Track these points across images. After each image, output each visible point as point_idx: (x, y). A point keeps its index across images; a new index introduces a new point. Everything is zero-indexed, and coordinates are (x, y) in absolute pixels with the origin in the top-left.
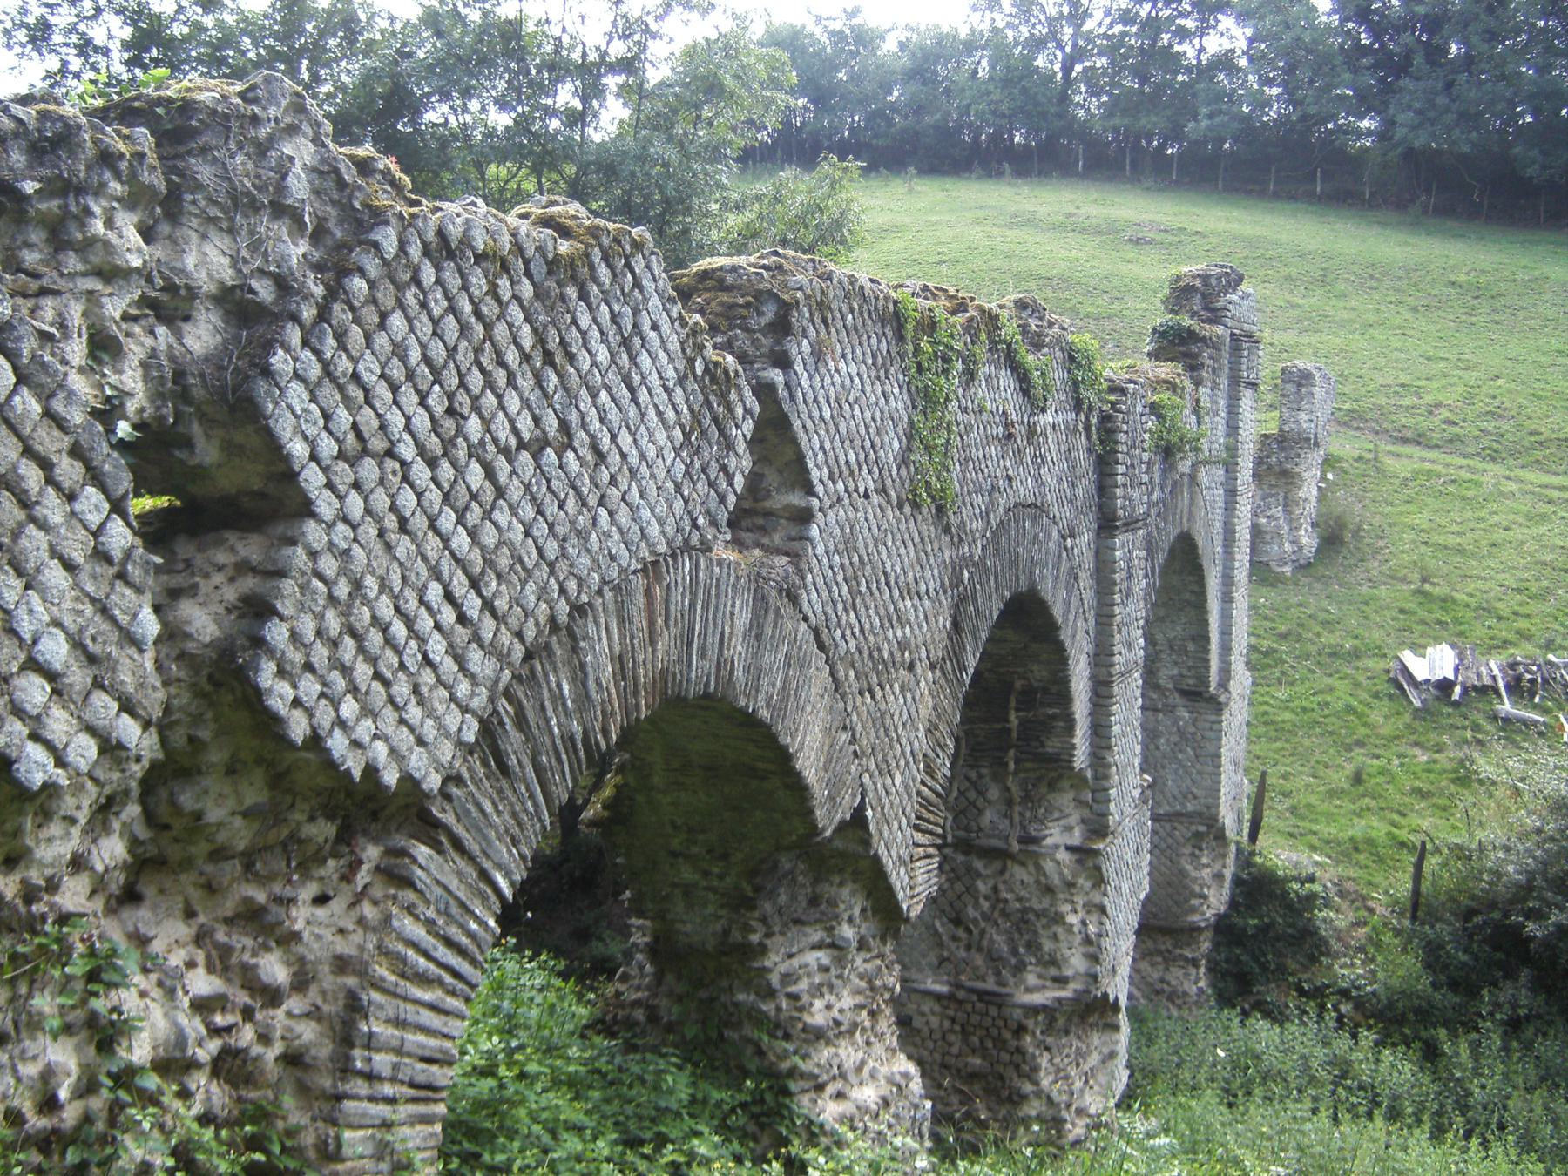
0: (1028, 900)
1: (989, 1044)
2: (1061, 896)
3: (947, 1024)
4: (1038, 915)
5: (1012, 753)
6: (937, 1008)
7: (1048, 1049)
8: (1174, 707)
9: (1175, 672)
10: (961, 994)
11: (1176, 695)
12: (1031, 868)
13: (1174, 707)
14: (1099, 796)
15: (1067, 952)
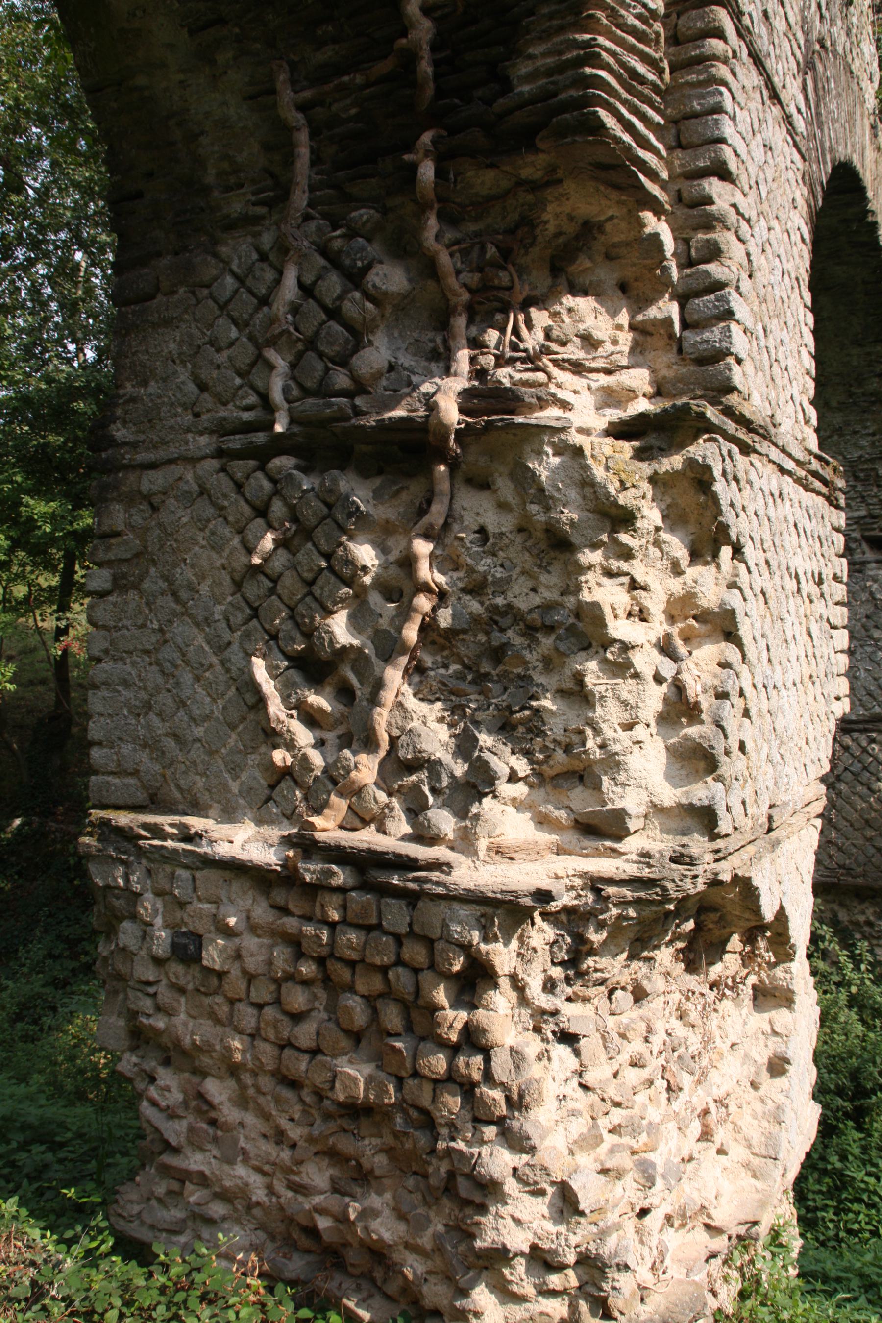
0: (502, 586)
1: (392, 1017)
2: (591, 557)
3: (281, 955)
4: (530, 631)
5: (427, 138)
6: (262, 912)
7: (568, 1038)
8: (864, 563)
9: (863, 513)
10: (310, 871)
11: (865, 546)
12: (506, 488)
13: (864, 563)
14: (705, 303)
15: (620, 741)
